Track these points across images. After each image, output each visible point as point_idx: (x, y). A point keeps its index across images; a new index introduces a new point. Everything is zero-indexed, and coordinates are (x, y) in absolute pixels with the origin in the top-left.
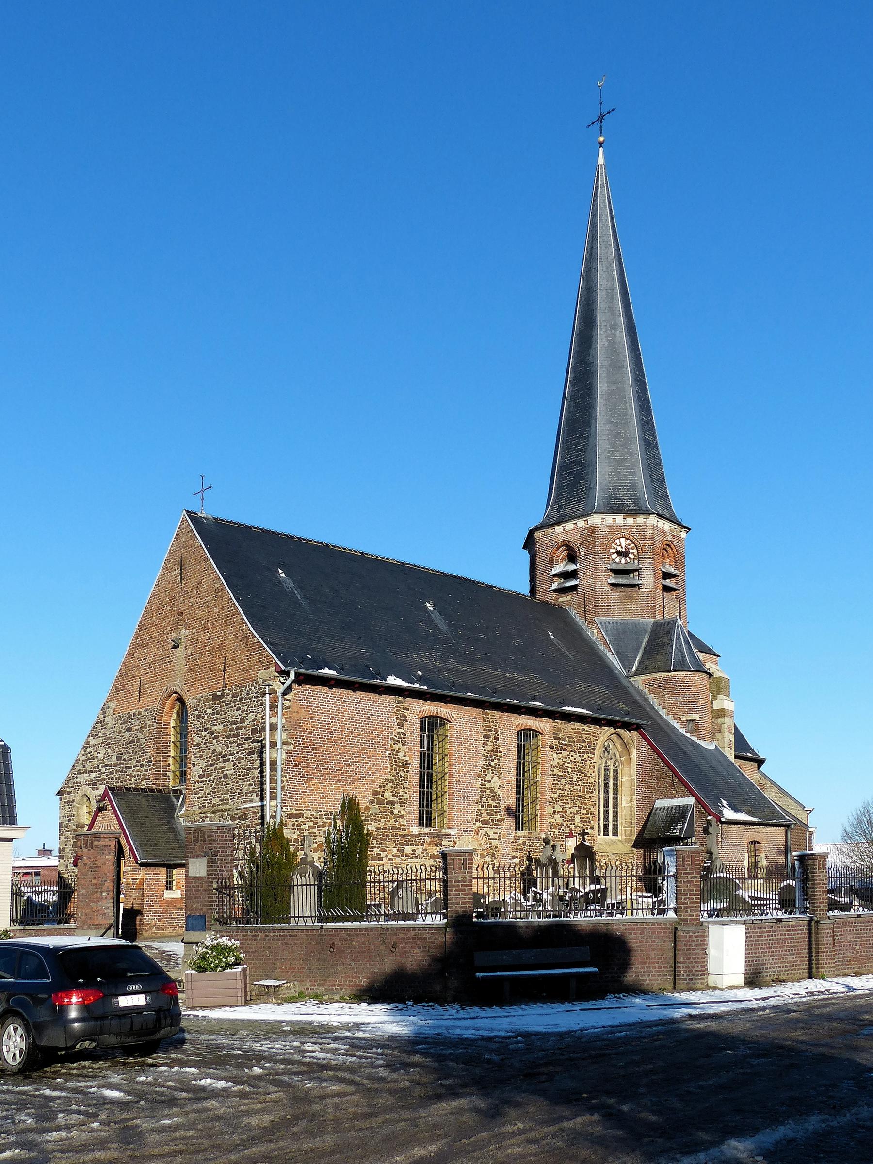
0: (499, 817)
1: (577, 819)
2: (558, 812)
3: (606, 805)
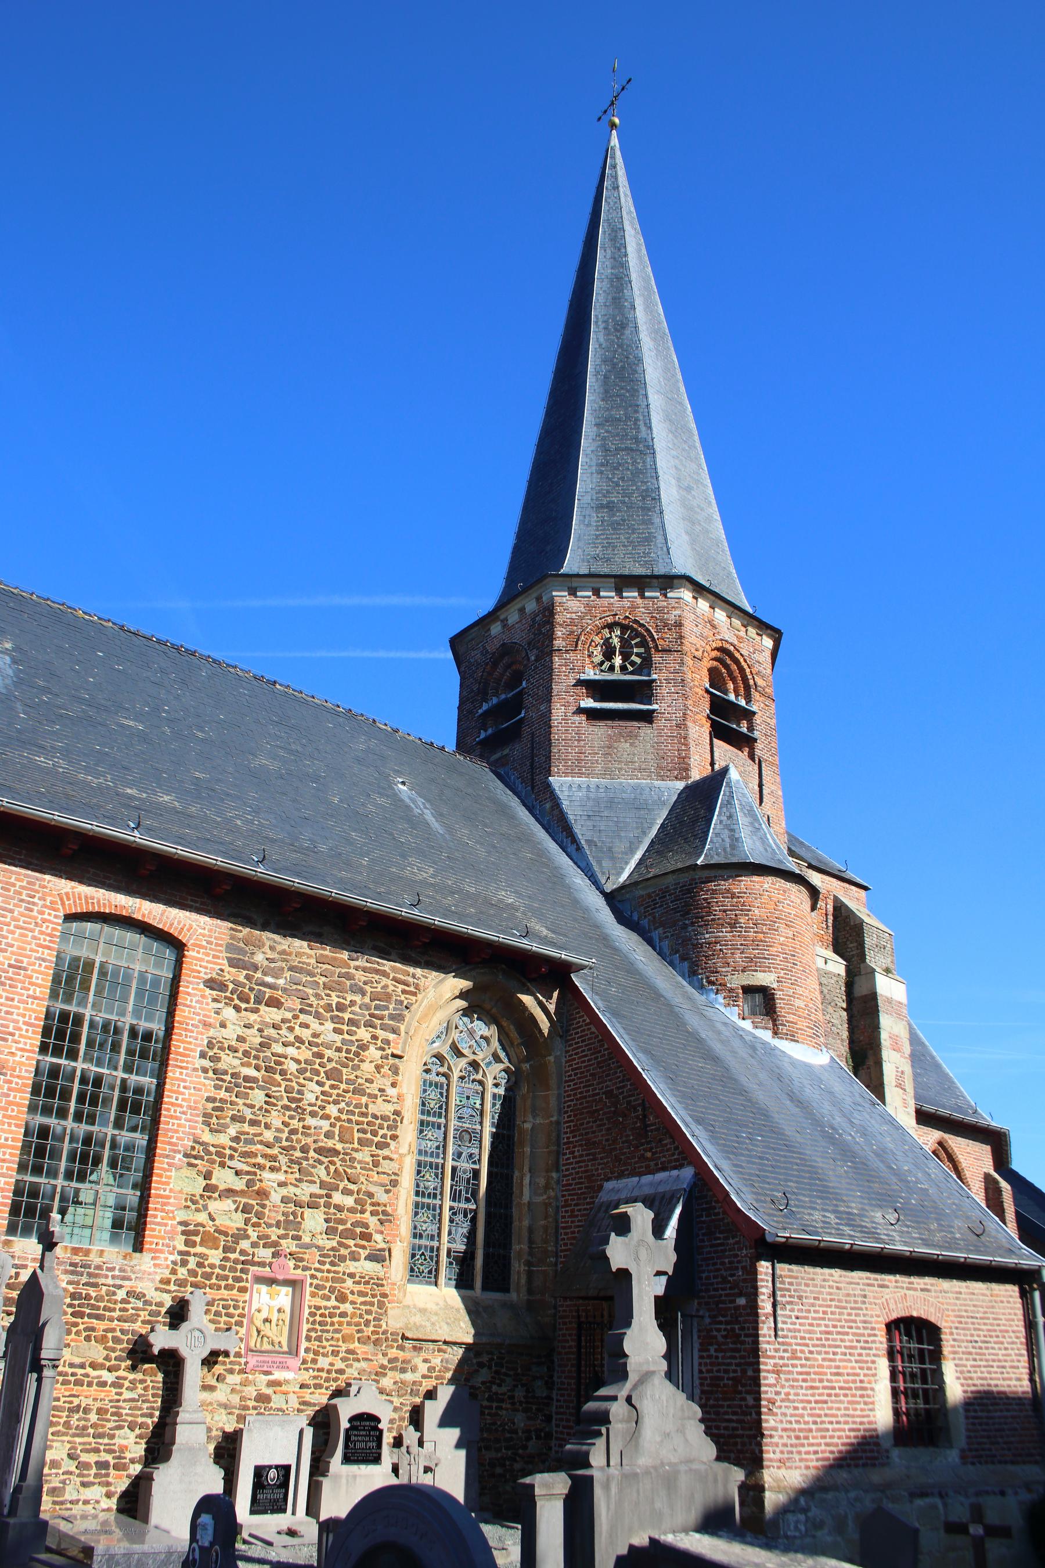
1: (314, 1221)
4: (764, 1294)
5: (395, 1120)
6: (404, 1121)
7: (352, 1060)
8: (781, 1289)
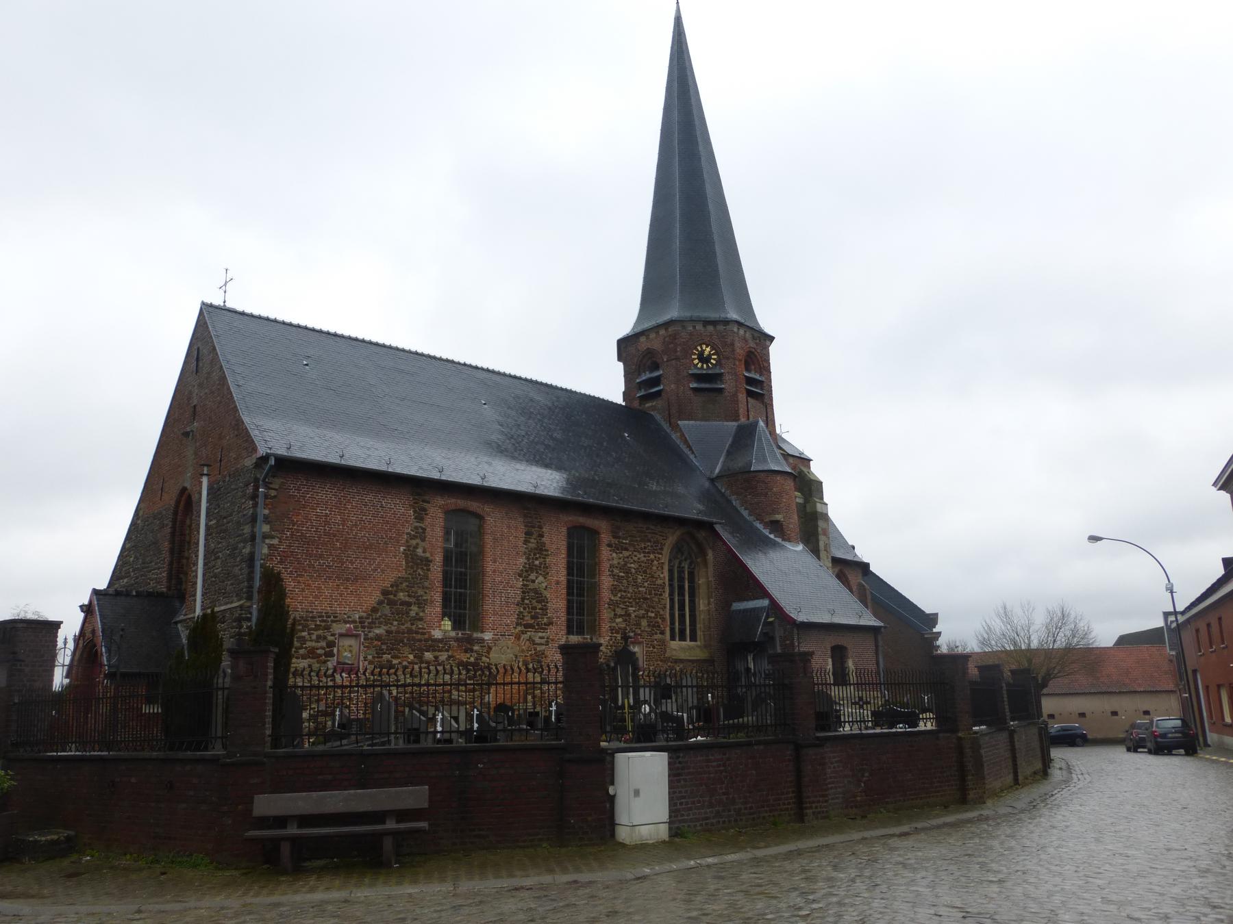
1: (644, 623)
2: (621, 616)
3: (682, 608)
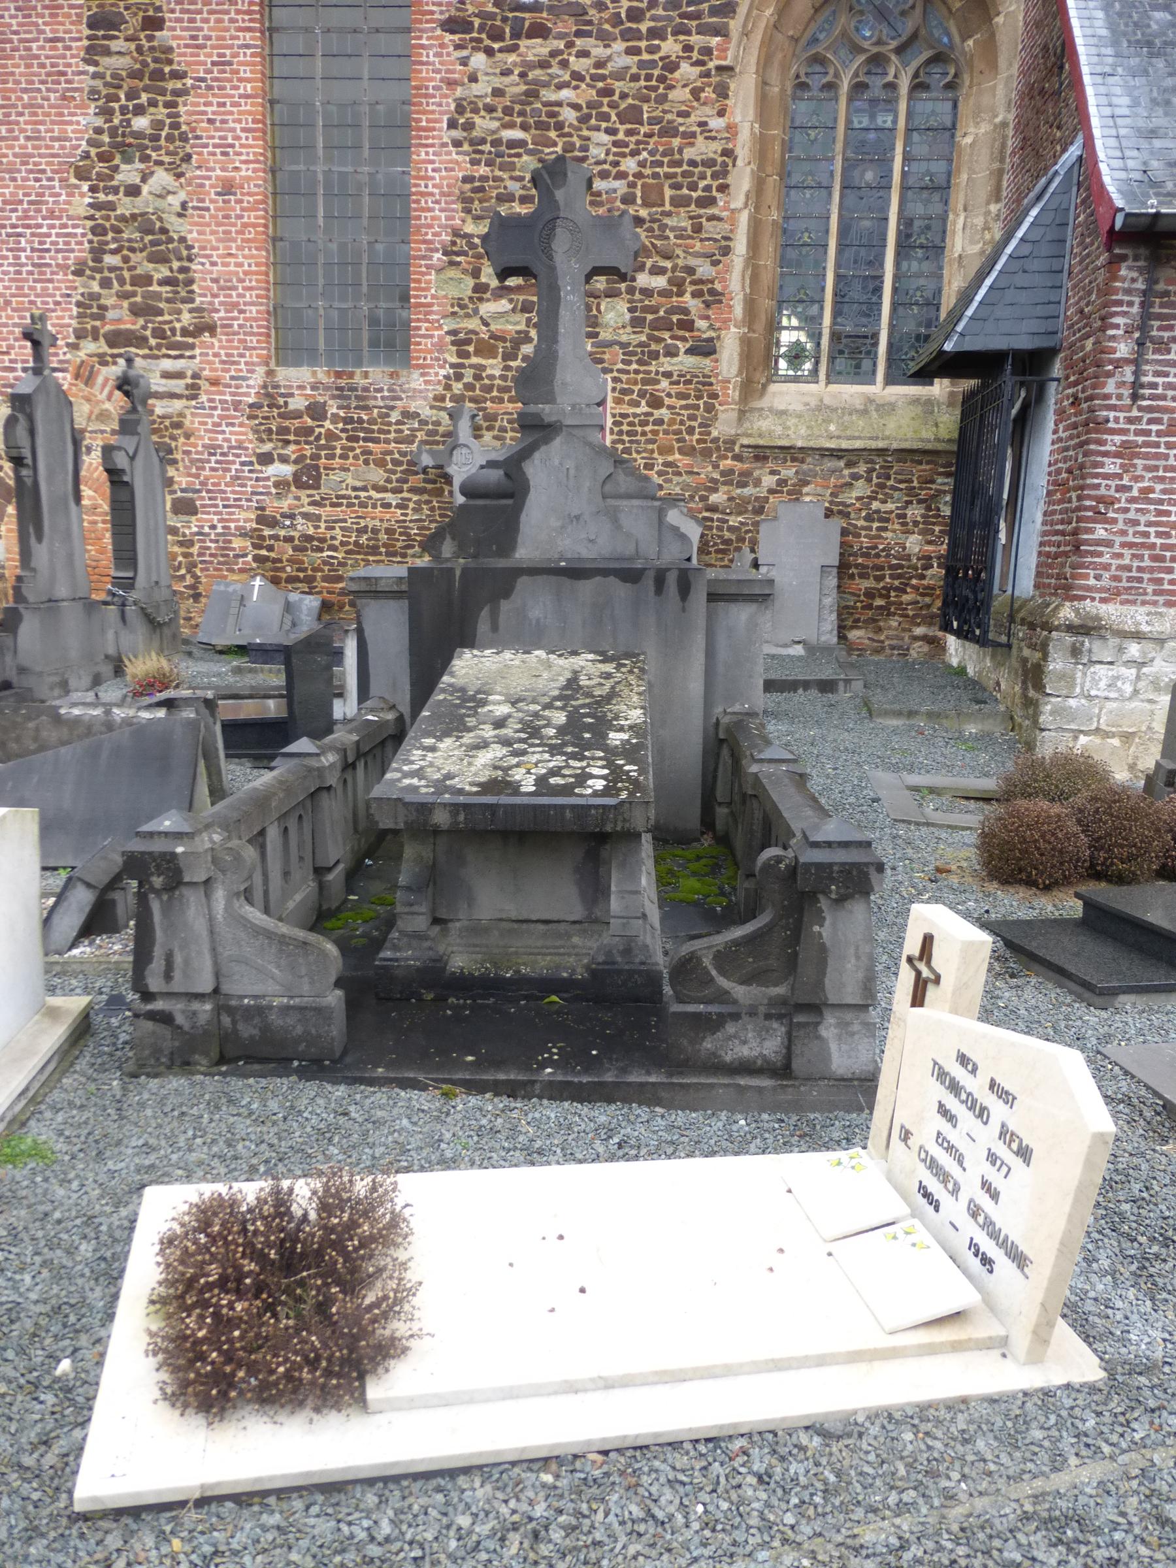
0: (186, 318)
4: (1117, 326)
5: (724, 164)
6: (739, 163)
7: (655, 89)
8: (1160, 317)
